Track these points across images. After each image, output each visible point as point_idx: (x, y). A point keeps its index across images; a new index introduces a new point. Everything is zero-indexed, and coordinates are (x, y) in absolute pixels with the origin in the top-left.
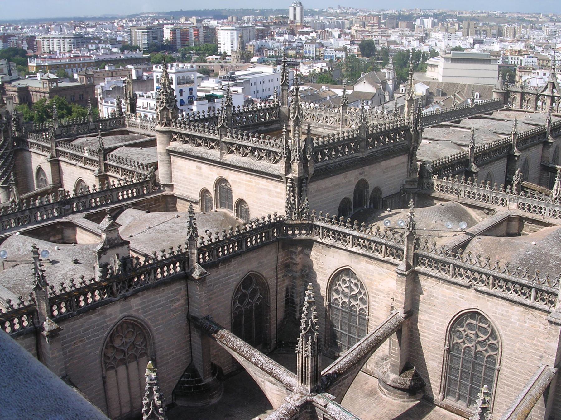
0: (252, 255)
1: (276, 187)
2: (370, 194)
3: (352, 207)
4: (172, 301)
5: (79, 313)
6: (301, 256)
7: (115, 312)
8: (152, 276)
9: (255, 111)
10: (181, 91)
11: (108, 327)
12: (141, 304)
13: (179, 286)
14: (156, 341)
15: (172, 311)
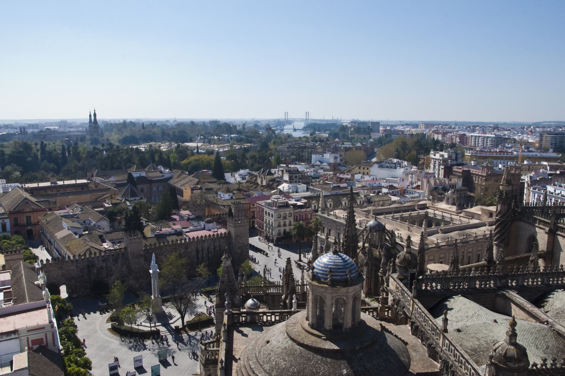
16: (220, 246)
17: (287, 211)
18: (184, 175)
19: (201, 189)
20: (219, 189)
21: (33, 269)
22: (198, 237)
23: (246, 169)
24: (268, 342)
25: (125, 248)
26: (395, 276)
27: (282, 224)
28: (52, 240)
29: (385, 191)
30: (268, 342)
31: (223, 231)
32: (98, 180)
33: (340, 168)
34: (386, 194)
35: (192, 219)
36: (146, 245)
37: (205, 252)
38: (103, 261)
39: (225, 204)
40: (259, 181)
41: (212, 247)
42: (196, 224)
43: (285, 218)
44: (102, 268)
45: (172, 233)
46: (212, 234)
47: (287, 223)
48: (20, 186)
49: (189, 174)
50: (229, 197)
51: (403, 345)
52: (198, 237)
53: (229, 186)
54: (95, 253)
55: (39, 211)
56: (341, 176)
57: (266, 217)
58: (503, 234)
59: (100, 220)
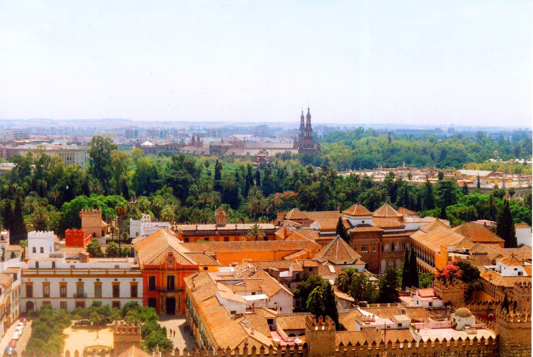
18: (441, 228)
19: (467, 253)
20: (500, 256)
22: (437, 340)
25: (305, 346)
31: (487, 333)
36: (341, 344)
39: (506, 285)
45: (392, 327)
46: (464, 338)
48: (170, 226)
49: (453, 225)
50: (516, 273)
52: (437, 340)
53: (514, 250)
54: (254, 348)
55: (189, 269)
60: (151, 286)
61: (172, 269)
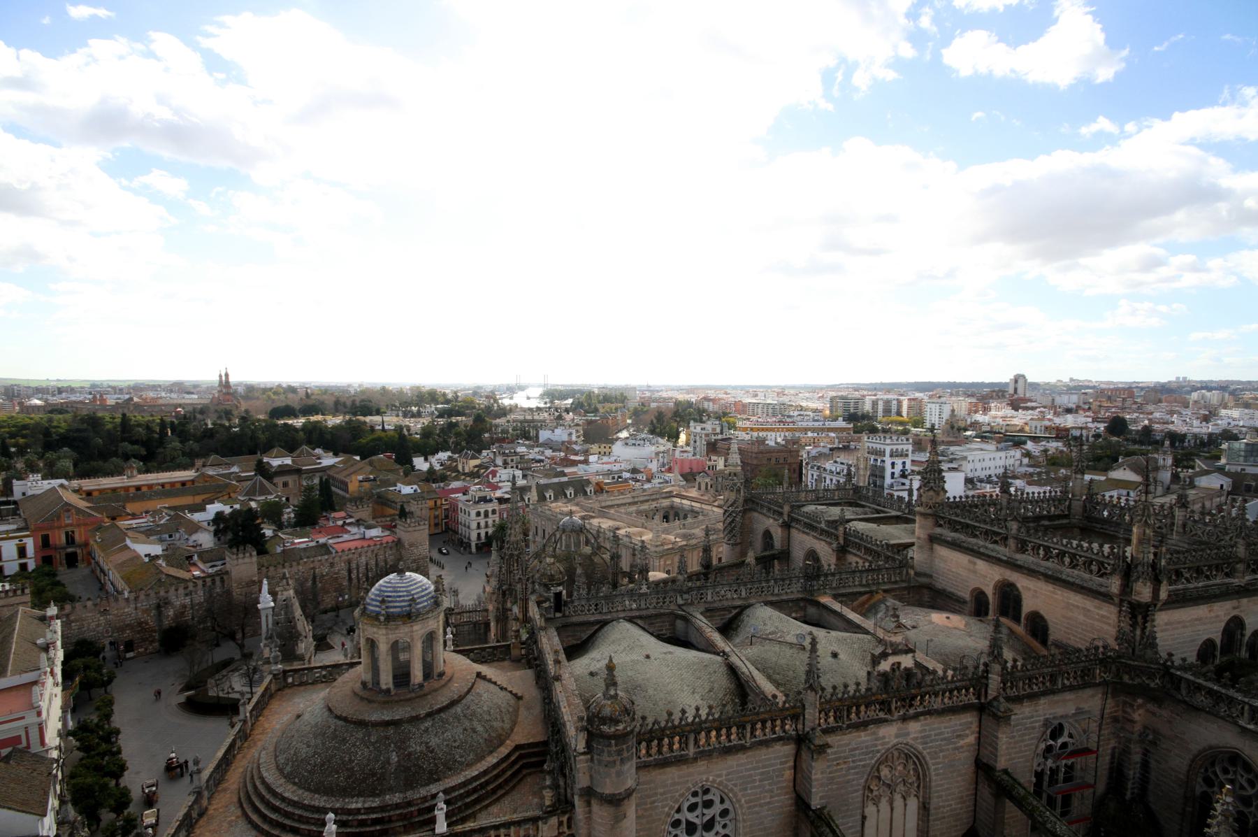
0: (1068, 696)
1: (1099, 608)
2: (1246, 638)
3: (1218, 653)
4: (958, 736)
5: (849, 727)
6: (1141, 711)
7: (889, 734)
8: (939, 699)
9: (1037, 502)
10: (893, 464)
11: (878, 751)
12: (921, 732)
13: (970, 718)
14: (933, 784)
15: (957, 748)
16: (386, 561)
17: (490, 507)
19: (375, 480)
21: (43, 619)
23: (445, 449)
24: (299, 716)
26: (533, 598)
27: (483, 524)
28: (106, 568)
29: (626, 475)
30: (299, 716)
31: (390, 539)
32: (211, 472)
33: (574, 446)
34: (626, 480)
35: (350, 524)
37: (362, 569)
38: (186, 595)
40: (460, 468)
41: (373, 562)
42: (354, 530)
43: (486, 515)
44: (184, 606)
47: (490, 522)
51: (513, 702)
56: (572, 457)
57: (462, 517)
58: (733, 529)
59: (196, 532)
60: (45, 542)
61: (71, 525)
